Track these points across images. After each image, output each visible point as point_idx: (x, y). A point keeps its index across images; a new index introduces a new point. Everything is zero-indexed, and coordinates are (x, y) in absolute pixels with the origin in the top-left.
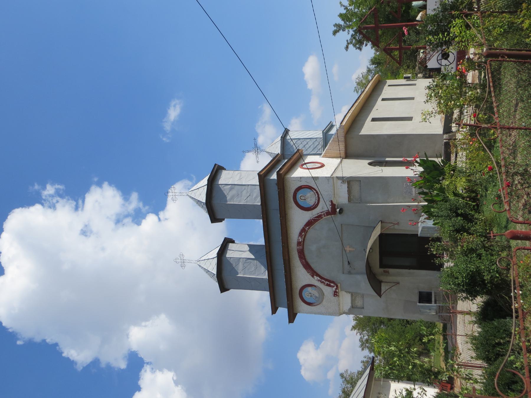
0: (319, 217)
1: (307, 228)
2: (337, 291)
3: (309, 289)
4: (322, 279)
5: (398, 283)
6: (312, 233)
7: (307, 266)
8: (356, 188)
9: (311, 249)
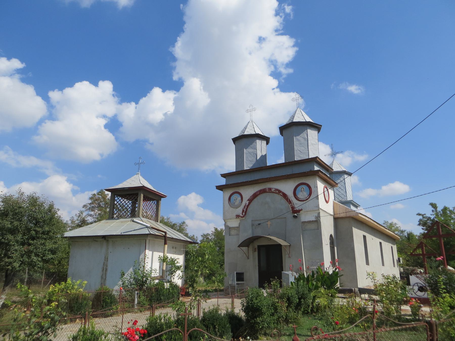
0: (290, 202)
1: (282, 194)
2: (240, 217)
3: (240, 198)
4: (247, 206)
5: (248, 258)
6: (278, 197)
7: (255, 196)
8: (313, 226)
9: (267, 197)
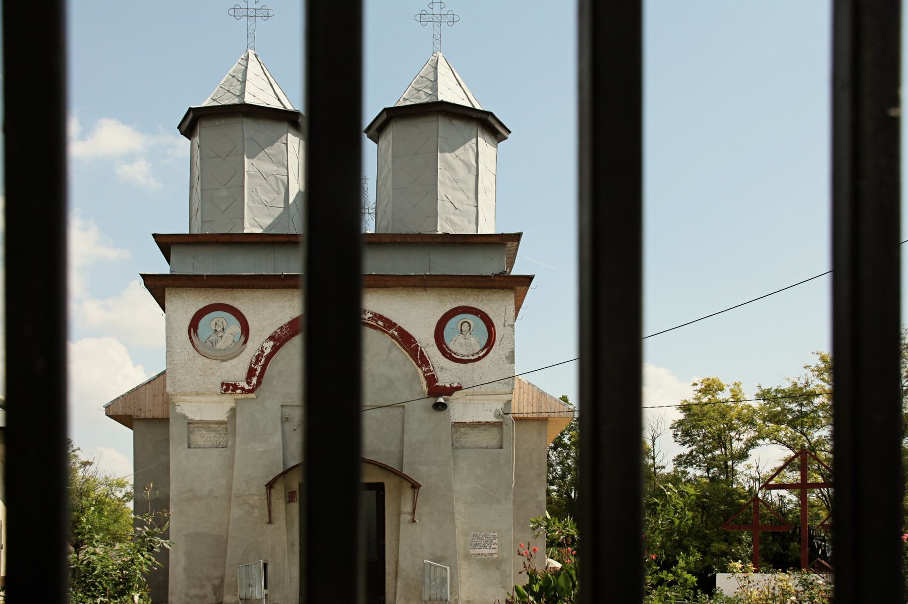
0: (422, 360)
1: (396, 333)
2: (239, 391)
3: (235, 327)
